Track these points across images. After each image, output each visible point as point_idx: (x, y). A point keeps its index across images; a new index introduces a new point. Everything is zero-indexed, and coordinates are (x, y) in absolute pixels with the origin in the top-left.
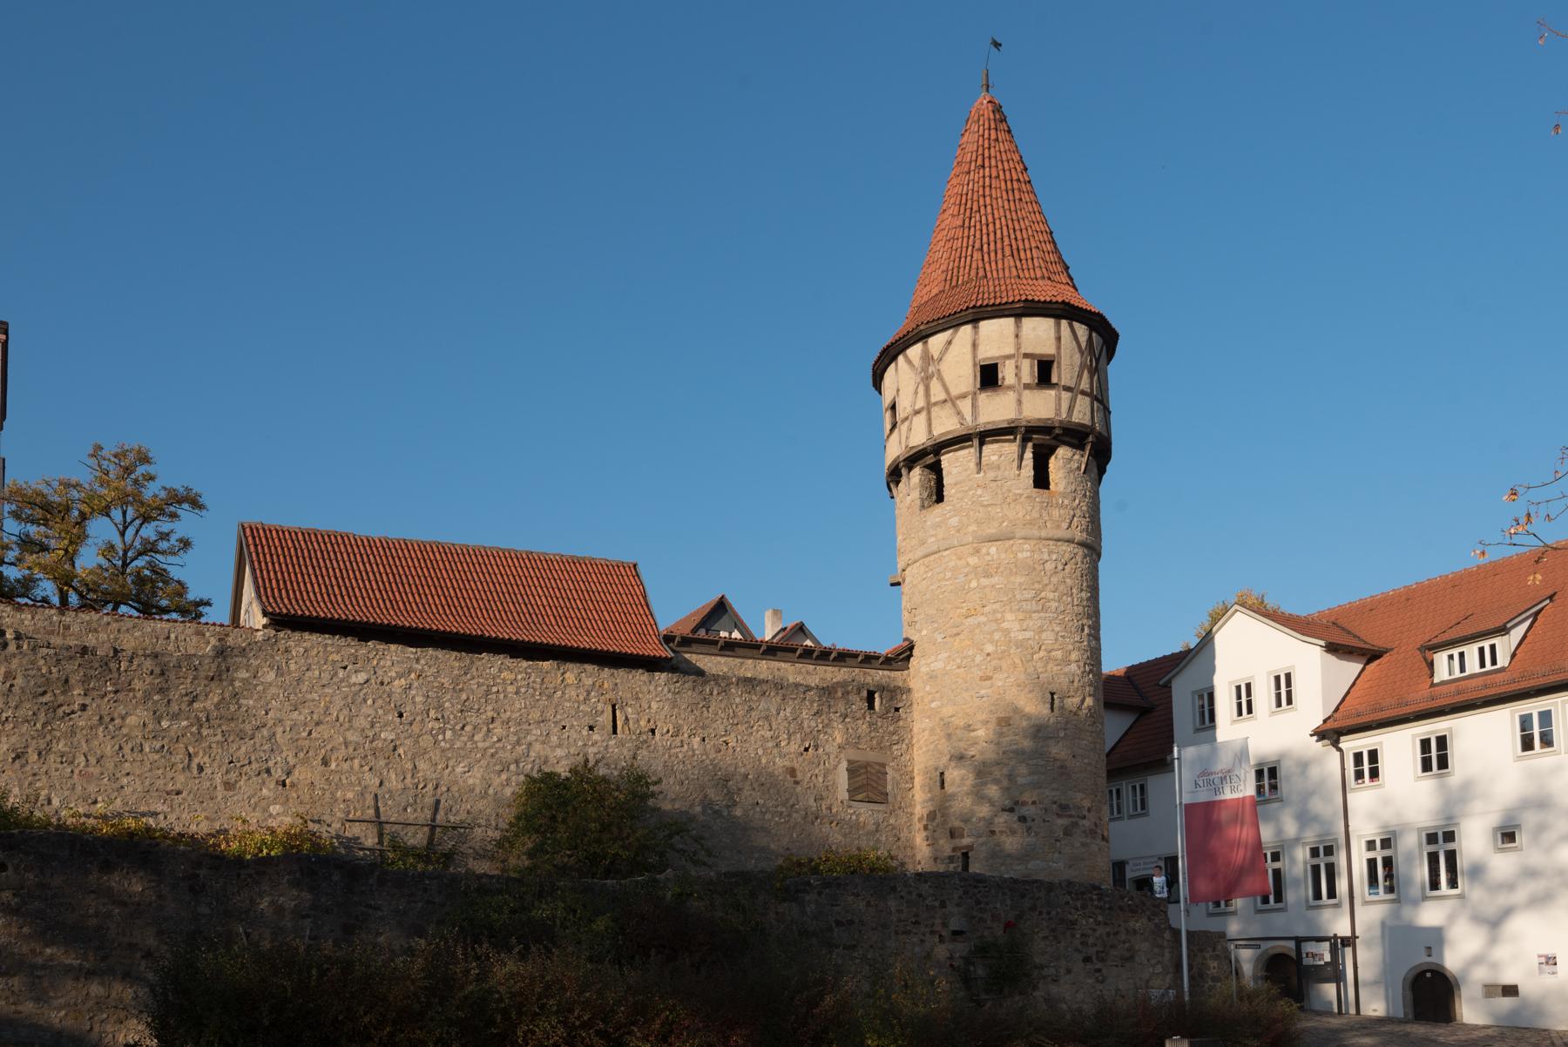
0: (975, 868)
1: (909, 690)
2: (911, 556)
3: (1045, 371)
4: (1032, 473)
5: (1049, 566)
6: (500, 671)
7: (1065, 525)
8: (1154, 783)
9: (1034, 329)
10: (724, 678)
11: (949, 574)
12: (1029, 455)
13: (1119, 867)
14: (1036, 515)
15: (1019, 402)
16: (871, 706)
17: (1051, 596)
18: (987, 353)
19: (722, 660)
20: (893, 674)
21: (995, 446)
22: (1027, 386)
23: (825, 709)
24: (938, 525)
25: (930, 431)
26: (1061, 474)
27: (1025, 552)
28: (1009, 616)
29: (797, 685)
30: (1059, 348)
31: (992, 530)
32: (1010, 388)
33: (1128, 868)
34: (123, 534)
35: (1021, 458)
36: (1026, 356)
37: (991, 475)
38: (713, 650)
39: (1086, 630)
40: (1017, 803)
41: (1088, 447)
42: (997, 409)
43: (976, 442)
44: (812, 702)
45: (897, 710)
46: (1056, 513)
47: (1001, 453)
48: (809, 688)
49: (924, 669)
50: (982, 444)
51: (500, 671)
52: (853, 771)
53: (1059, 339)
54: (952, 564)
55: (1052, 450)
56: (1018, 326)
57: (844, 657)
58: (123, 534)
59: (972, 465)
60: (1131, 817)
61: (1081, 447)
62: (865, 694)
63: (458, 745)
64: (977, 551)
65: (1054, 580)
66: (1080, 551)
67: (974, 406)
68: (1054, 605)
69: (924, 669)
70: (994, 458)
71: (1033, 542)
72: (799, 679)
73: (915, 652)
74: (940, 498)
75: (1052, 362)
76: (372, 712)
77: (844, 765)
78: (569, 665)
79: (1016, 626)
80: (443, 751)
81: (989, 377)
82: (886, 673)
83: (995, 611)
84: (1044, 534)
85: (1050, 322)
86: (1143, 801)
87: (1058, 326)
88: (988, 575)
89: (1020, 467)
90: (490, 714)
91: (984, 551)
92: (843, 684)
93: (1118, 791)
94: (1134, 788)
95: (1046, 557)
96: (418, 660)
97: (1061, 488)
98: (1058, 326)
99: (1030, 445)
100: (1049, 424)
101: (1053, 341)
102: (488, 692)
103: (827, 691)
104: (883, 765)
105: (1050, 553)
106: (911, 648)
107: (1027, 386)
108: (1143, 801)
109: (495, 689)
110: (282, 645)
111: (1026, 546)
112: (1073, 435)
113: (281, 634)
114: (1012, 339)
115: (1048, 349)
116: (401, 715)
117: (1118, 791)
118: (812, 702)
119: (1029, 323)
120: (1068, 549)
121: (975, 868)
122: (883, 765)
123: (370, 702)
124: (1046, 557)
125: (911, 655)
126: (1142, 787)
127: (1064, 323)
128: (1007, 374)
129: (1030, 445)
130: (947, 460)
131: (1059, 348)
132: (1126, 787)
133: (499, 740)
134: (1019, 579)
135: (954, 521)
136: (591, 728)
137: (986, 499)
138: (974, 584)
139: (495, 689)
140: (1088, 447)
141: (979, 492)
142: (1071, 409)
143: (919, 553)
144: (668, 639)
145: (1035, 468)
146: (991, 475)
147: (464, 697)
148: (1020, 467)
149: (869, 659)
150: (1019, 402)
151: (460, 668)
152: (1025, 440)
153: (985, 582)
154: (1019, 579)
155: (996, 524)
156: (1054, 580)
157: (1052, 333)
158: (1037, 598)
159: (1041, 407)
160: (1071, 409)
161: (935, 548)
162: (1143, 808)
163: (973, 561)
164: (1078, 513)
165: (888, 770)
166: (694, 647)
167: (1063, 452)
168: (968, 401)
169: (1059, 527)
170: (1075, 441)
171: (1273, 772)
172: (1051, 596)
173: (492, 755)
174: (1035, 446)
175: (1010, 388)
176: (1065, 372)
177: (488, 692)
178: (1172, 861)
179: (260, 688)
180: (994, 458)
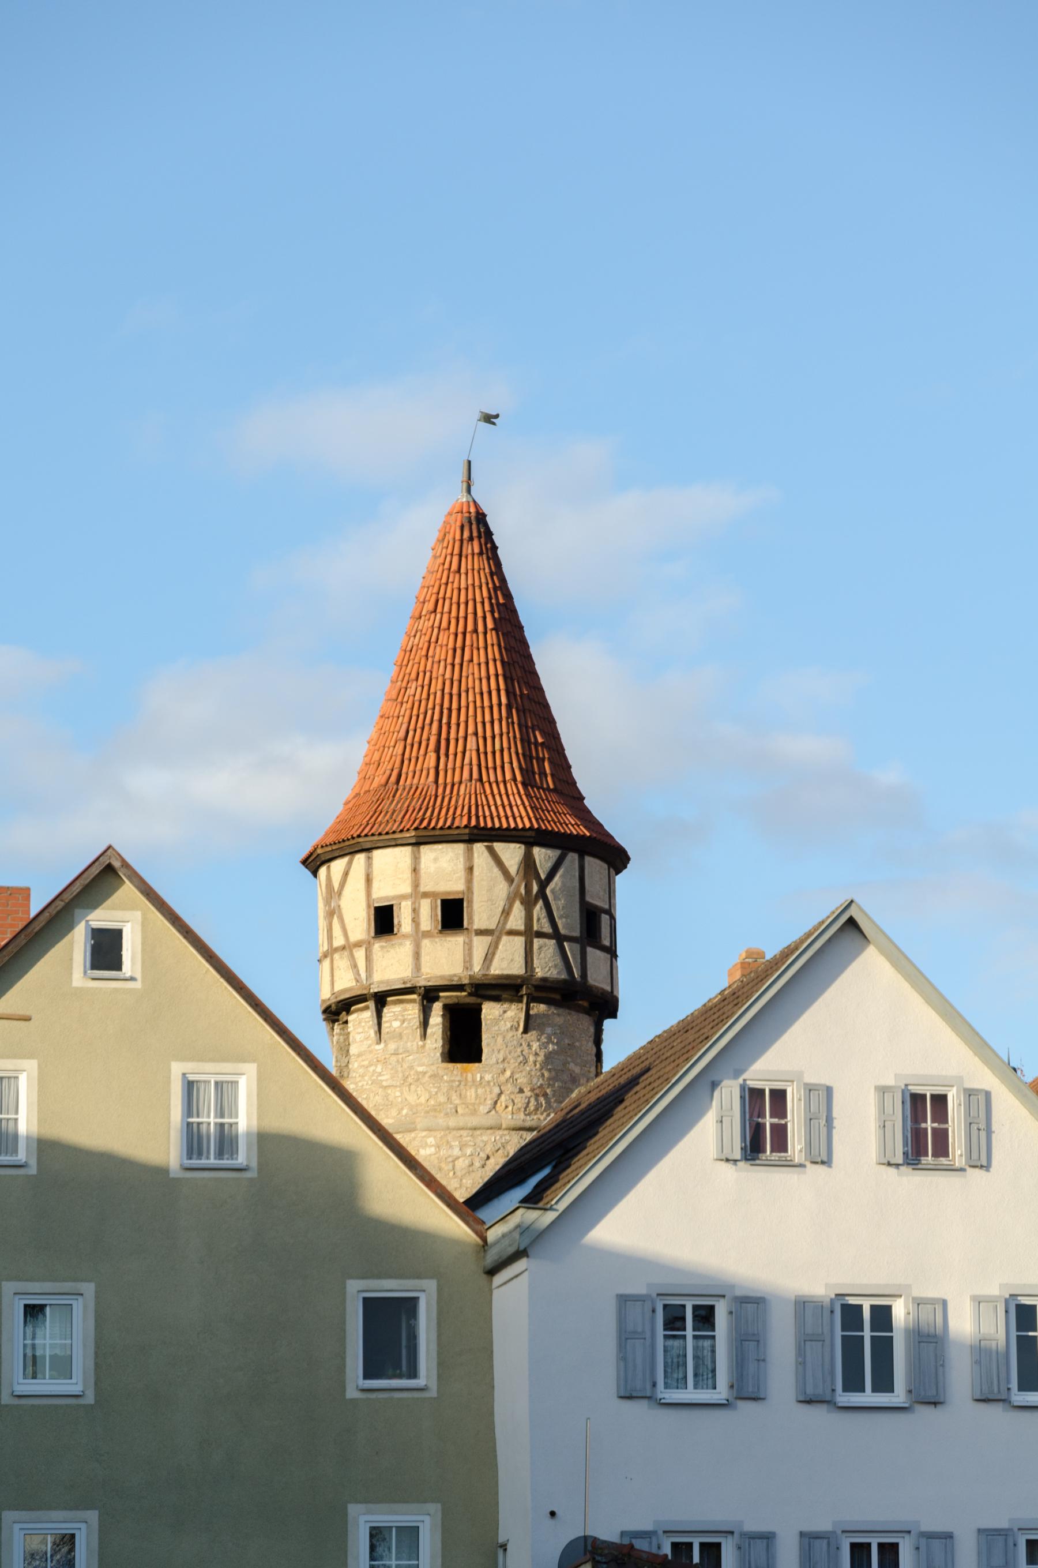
3: (452, 914)
4: (440, 1043)
5: (462, 1164)
7: (483, 1109)
9: (436, 860)
12: (437, 1018)
14: (442, 1099)
15: (417, 955)
18: (384, 892)
22: (427, 934)
30: (469, 881)
32: (405, 936)
35: (425, 1024)
36: (425, 895)
37: (392, 1046)
42: (392, 964)
43: (371, 1004)
46: (471, 1094)
53: (470, 869)
67: (368, 959)
71: (439, 1134)
81: (384, 920)
84: (452, 1122)
85: (460, 848)
87: (469, 856)
89: (424, 1035)
95: (456, 1152)
98: (469, 856)
99: (437, 1008)
107: (427, 934)
111: (431, 1140)
114: (408, 875)
115: (454, 886)
119: (430, 854)
124: (456, 1152)
127: (479, 848)
128: (403, 919)
131: (469, 881)
142: (489, 958)
146: (392, 1046)
148: (424, 1035)
150: (417, 955)
155: (394, 1112)
157: (461, 865)
160: (489, 958)
168: (360, 954)
169: (474, 1112)
174: (447, 1008)
175: (405, 936)
176: (481, 913)
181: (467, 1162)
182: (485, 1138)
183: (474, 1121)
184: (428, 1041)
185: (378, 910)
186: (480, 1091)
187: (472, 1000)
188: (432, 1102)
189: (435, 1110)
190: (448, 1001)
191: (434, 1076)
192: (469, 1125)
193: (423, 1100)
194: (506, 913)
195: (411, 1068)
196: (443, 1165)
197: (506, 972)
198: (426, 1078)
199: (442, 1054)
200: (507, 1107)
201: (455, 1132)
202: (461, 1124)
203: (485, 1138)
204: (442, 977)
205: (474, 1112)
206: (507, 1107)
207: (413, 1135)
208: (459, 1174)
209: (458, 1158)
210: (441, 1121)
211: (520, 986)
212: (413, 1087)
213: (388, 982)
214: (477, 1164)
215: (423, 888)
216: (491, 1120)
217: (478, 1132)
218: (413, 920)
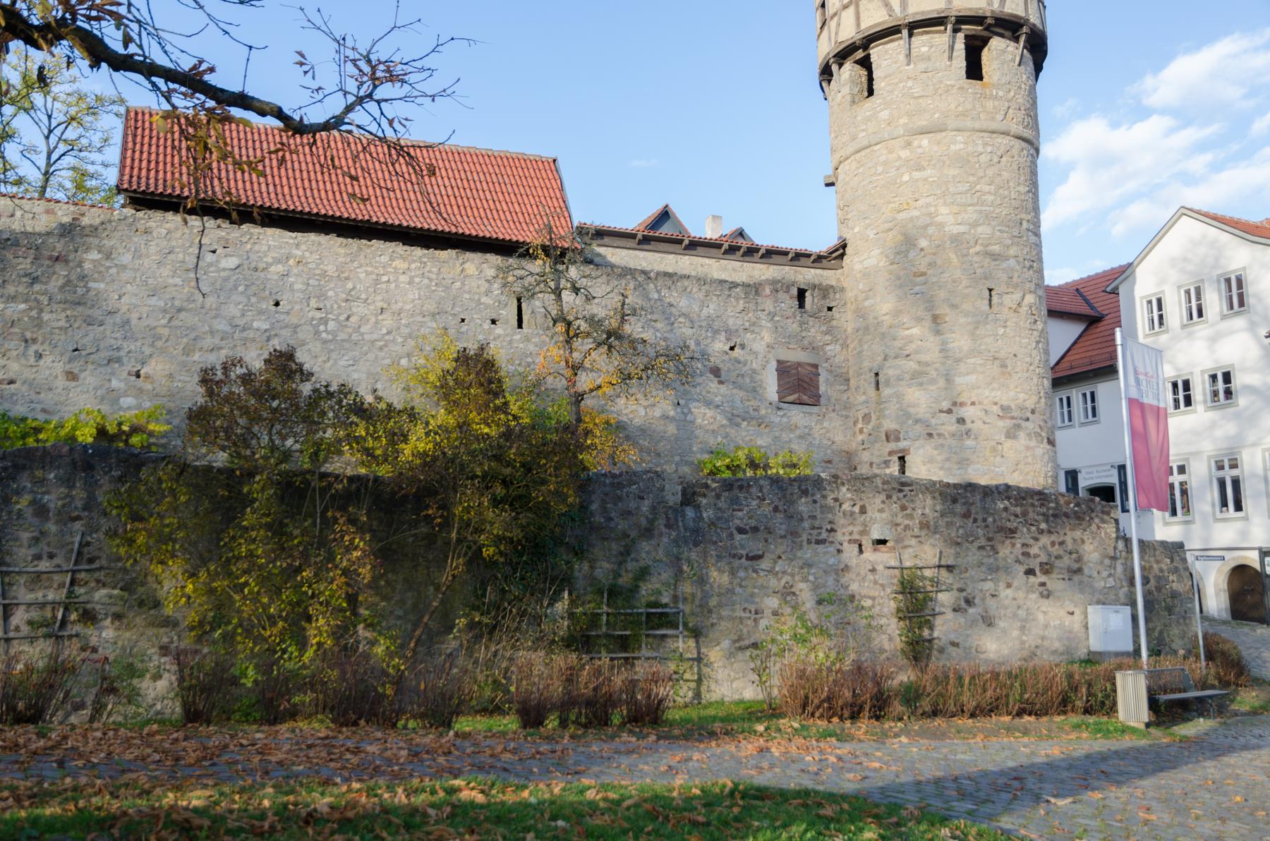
0: (911, 473)
1: (843, 290)
2: (843, 153)
4: (964, 64)
5: (983, 158)
6: (392, 259)
7: (999, 117)
8: (1103, 389)
10: (644, 272)
11: (880, 169)
12: (960, 45)
13: (1072, 476)
16: (801, 305)
17: (987, 188)
19: (641, 254)
20: (826, 273)
21: (925, 37)
23: (752, 306)
24: (868, 120)
25: (858, 25)
26: (995, 64)
27: (958, 143)
29: (722, 282)
31: (922, 122)
33: (1080, 477)
34: (47, 138)
35: (952, 48)
38: (632, 243)
39: (1025, 225)
40: (955, 404)
41: (1023, 39)
43: (905, 32)
44: (737, 299)
45: (830, 309)
46: (990, 105)
47: (933, 44)
48: (734, 285)
49: (858, 267)
50: (911, 35)
51: (392, 259)
52: (783, 370)
54: (883, 158)
55: (985, 41)
57: (771, 254)
58: (47, 138)
59: (902, 57)
60: (1082, 424)
61: (1016, 40)
62: (795, 292)
63: (342, 336)
64: (909, 144)
65: (990, 172)
66: (1018, 144)
68: (990, 198)
69: (858, 267)
70: (924, 49)
72: (724, 276)
73: (848, 250)
74: (871, 92)
76: (245, 300)
77: (774, 365)
78: (469, 255)
79: (951, 219)
80: (325, 342)
82: (818, 271)
83: (928, 205)
84: (977, 125)
86: (1094, 409)
88: (920, 168)
89: (950, 58)
90: (380, 305)
91: (916, 143)
92: (774, 282)
93: (1068, 399)
94: (1084, 395)
95: (980, 149)
96: (298, 245)
97: (995, 78)
99: (960, 36)
100: (980, 13)
102: (377, 282)
103: (753, 289)
104: (816, 366)
105: (985, 144)
106: (844, 246)
108: (1094, 409)
109: (385, 278)
110: (141, 225)
111: (959, 138)
112: (1009, 26)
113: (140, 214)
116: (277, 304)
117: (1068, 399)
118: (737, 299)
121: (911, 473)
122: (816, 366)
123: (241, 289)
125: (842, 255)
126: (1093, 394)
129: (960, 36)
130: (876, 52)
132: (1076, 394)
133: (389, 333)
135: (884, 115)
136: (493, 322)
137: (917, 90)
138: (906, 178)
139: (385, 278)
140: (1023, 39)
141: (910, 83)
143: (850, 149)
144: (582, 231)
145: (967, 59)
147: (350, 285)
148: (950, 58)
149: (799, 257)
151: (346, 255)
152: (956, 31)
153: (917, 175)
156: (990, 172)
161: (865, 143)
162: (1094, 415)
163: (905, 154)
164: (1014, 105)
165: (820, 370)
166: (607, 240)
167: (996, 43)
169: (993, 119)
170: (1008, 33)
171: (1227, 377)
172: (987, 188)
173: (381, 349)
174: (966, 37)
177: (377, 282)
178: (1122, 468)
179: (113, 271)
180: (924, 49)
183: (994, 126)
184: (954, 62)
186: (996, 103)
188: (961, 109)
191: (961, 88)
193: (953, 106)
195: (941, 82)
198: (954, 91)
199: (967, 72)
202: (984, 127)
204: (970, 9)
205: (993, 119)
210: (969, 123)
212: (944, 97)
213: (923, 13)
214: (996, 159)
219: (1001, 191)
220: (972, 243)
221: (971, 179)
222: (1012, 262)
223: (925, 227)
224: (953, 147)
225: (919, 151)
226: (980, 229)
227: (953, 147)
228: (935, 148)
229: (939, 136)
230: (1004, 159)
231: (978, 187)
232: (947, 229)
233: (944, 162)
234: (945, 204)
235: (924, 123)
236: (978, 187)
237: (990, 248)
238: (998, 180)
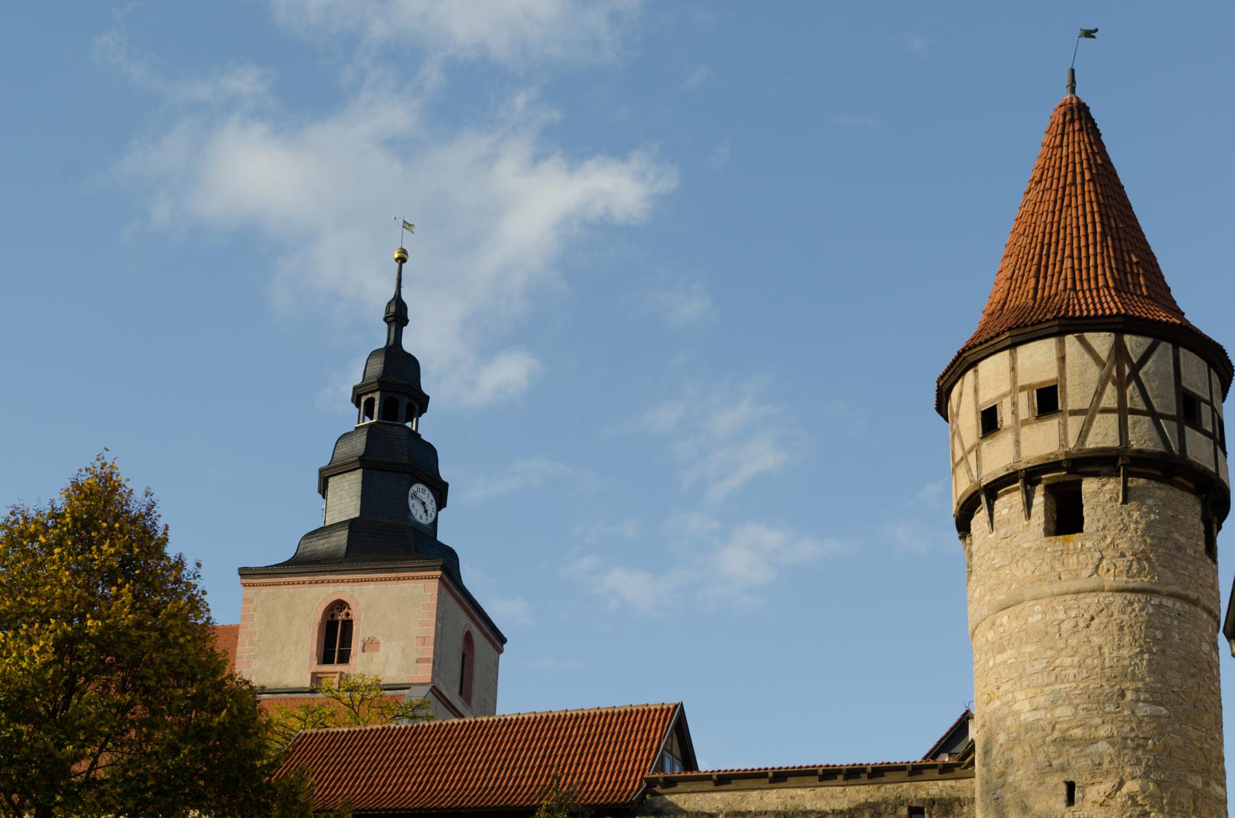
4: (1043, 519)
5: (1067, 626)
7: (1085, 573)
9: (1031, 356)
12: (1039, 499)
14: (1046, 568)
15: (1017, 443)
17: (1068, 661)
27: (1035, 615)
28: (1020, 695)
35: (1028, 505)
36: (1023, 388)
42: (998, 457)
46: (1072, 561)
56: (1013, 358)
67: (978, 459)
68: (1072, 672)
70: (1005, 511)
71: (1044, 602)
75: (1055, 387)
81: (989, 421)
84: (1056, 589)
85: (1051, 343)
87: (1061, 348)
88: (1002, 650)
89: (1029, 516)
95: (1061, 615)
98: (1061, 348)
101: (1054, 364)
107: (1025, 423)
120: (1091, 602)
124: (1061, 615)
127: (1070, 340)
134: (1031, 648)
137: (997, 562)
142: (1083, 435)
146: (1002, 532)
148: (1029, 516)
150: (1017, 443)
153: (1000, 658)
154: (1031, 648)
155: (1005, 589)
156: (1073, 642)
158: (1051, 668)
159: (1043, 441)
169: (1077, 577)
172: (1068, 661)
174: (1047, 488)
176: (1075, 396)
181: (1072, 624)
182: (1088, 600)
183: (1077, 585)
184: (1032, 520)
185: (984, 413)
186: (1081, 557)
187: (1072, 478)
189: (1040, 580)
190: (1050, 482)
191: (1037, 549)
192: (1073, 589)
193: (1029, 573)
194: (1099, 393)
196: (1049, 629)
197: (1100, 445)
198: (1032, 553)
199: (1045, 530)
200: (1108, 570)
201: (1059, 598)
202: (1065, 590)
203: (1088, 600)
204: (1040, 458)
205: (1077, 577)
206: (1108, 570)
207: (1022, 606)
208: (1064, 635)
209: (1063, 621)
210: (1046, 589)
211: (1116, 458)
214: (1082, 625)
215: (1020, 383)
216: (1093, 582)
217: (1082, 595)
218: (1013, 413)
219: (1088, 661)
220: (1048, 729)
221: (1049, 653)
222: (1103, 746)
223: (1004, 719)
224: (1031, 620)
225: (1001, 629)
226: (1058, 712)
227: (1031, 620)
228: (1014, 624)
229: (1018, 608)
230: (1096, 621)
231: (1058, 662)
232: (1023, 717)
233: (1021, 639)
234: (1022, 688)
235: (1002, 597)
236: (1058, 662)
237: (1071, 732)
238: (1082, 650)
